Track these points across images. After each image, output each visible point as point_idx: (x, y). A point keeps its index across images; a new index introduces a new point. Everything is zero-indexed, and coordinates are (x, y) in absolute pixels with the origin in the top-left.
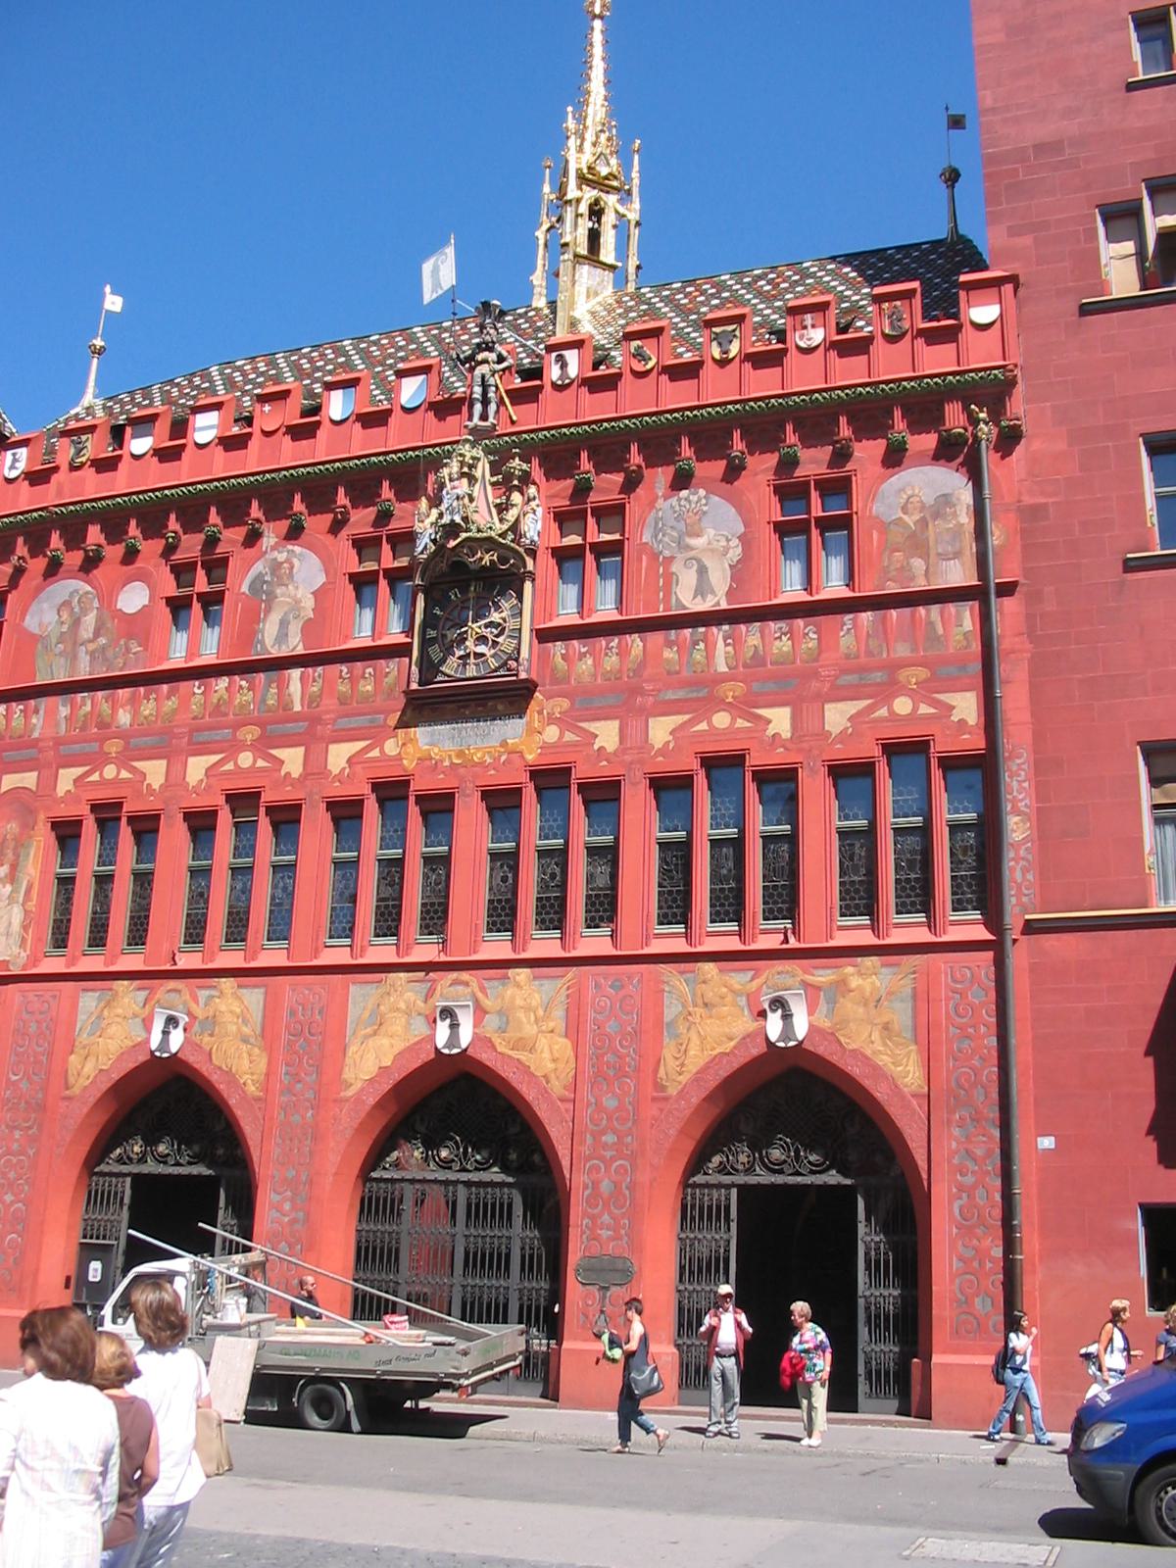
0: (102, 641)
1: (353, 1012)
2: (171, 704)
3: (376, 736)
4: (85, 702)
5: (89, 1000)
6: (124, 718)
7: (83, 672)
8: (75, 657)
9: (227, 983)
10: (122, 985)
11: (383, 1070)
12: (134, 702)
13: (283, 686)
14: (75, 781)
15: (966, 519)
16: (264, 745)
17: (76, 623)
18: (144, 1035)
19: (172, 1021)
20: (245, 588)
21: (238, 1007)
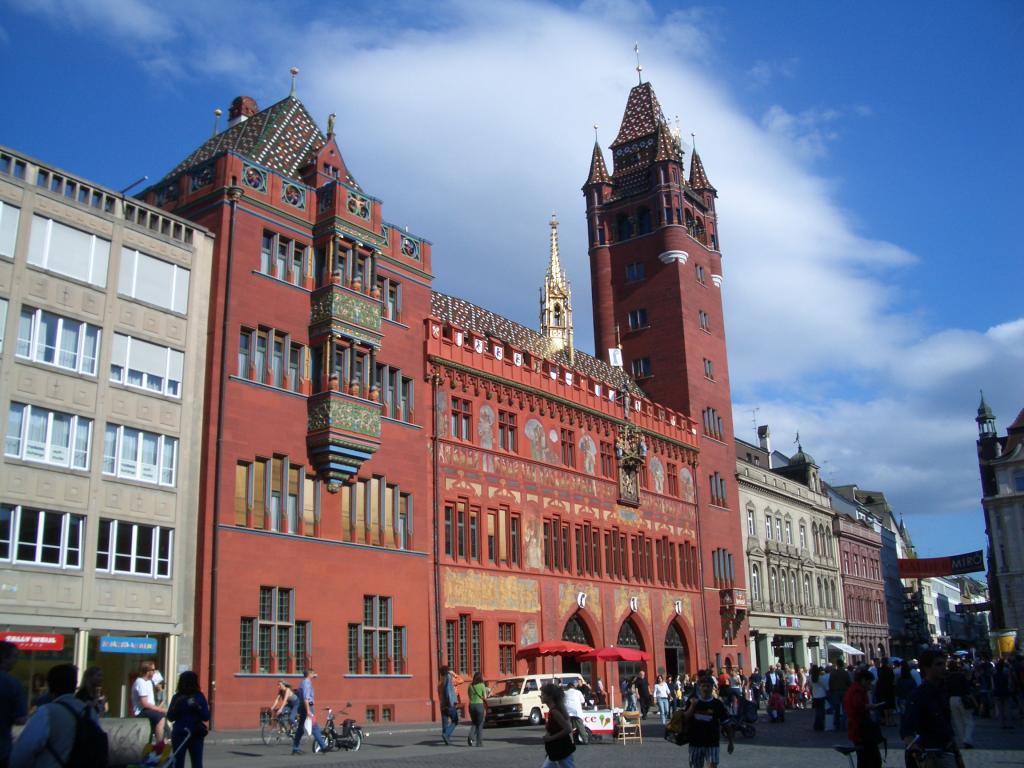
0: (548, 450)
1: (616, 598)
2: (568, 482)
3: (612, 510)
4: (548, 473)
5: (561, 587)
6: (557, 483)
7: (544, 460)
8: (541, 453)
9: (591, 584)
10: (569, 581)
11: (622, 616)
12: (558, 477)
13: (590, 483)
14: (549, 503)
15: (691, 485)
16: (591, 505)
17: (540, 438)
18: (574, 601)
19: (583, 596)
20: (580, 446)
21: (594, 591)
